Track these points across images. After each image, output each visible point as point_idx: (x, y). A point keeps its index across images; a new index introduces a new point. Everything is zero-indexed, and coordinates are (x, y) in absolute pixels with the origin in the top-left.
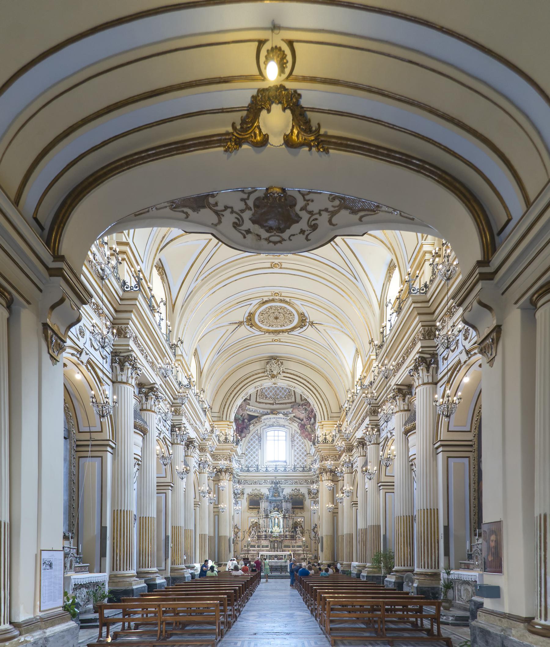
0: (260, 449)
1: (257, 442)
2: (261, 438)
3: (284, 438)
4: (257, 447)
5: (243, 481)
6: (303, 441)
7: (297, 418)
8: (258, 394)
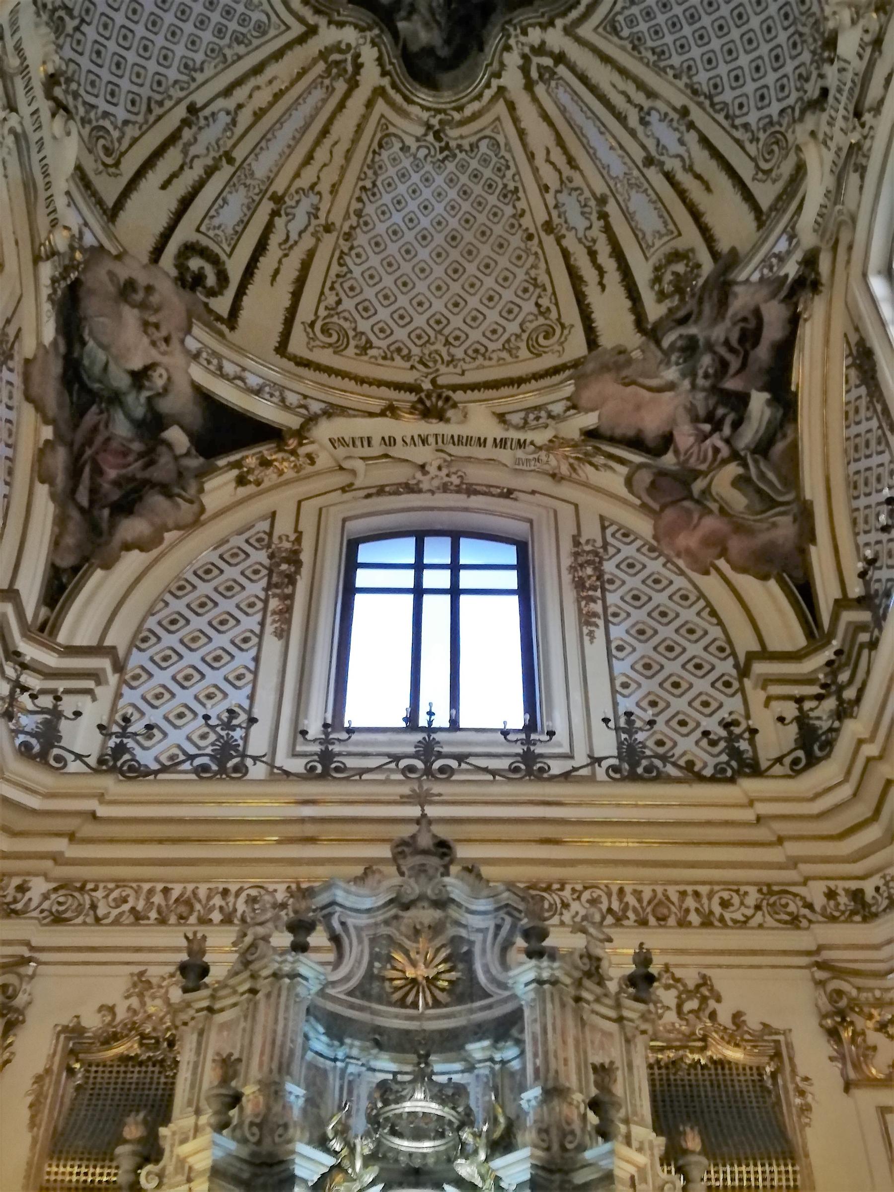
0: (283, 634)
1: (256, 588)
2: (298, 564)
3: (510, 579)
4: (251, 623)
5: (39, 887)
6: (680, 582)
7: (612, 440)
8: (305, 312)
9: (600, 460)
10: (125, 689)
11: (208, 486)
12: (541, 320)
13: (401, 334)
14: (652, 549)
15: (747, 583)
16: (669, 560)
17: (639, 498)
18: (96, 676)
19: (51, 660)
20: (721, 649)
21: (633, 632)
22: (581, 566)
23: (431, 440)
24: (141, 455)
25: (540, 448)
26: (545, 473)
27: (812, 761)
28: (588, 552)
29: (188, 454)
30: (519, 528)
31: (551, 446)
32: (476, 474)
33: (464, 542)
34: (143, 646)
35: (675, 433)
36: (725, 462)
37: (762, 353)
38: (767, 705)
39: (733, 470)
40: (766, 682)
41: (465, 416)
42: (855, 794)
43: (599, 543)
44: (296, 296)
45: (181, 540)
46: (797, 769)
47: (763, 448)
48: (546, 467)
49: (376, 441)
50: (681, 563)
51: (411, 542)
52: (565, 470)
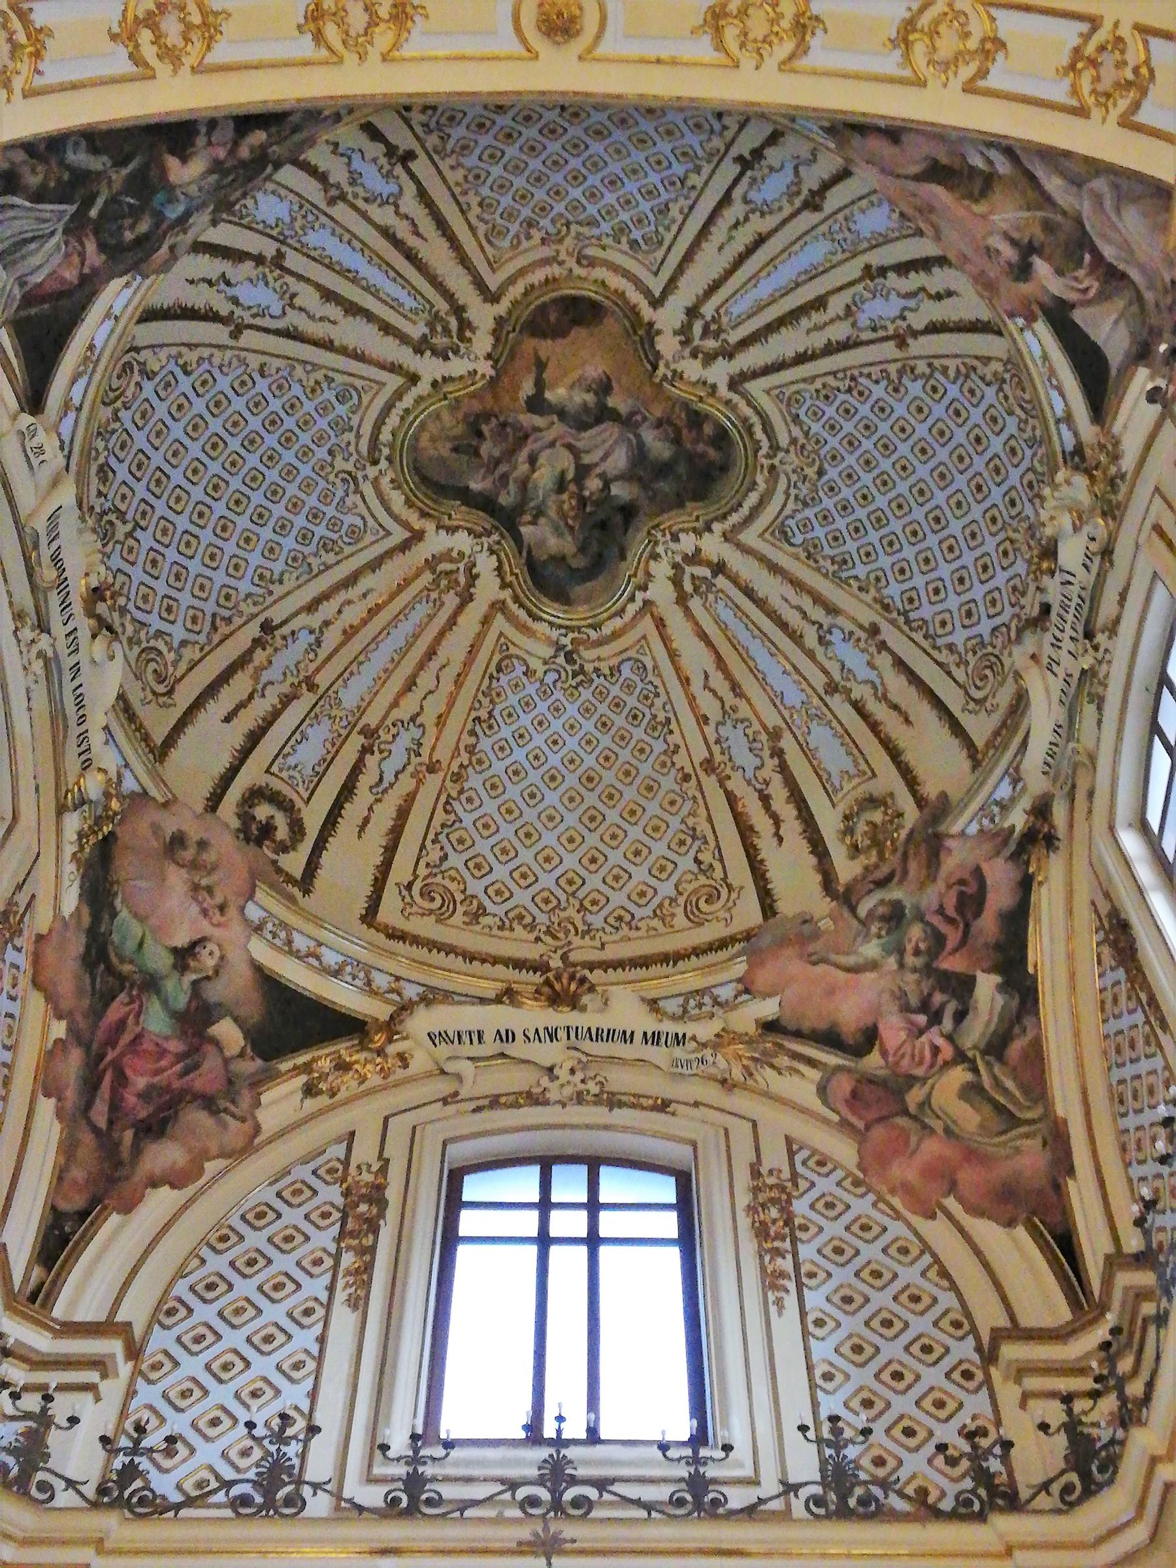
0: (359, 1303)
1: (324, 1239)
2: (382, 1204)
3: (668, 1224)
6: (897, 1229)
7: (798, 1035)
8: (401, 870)
9: (783, 1061)
10: (140, 1383)
11: (265, 1098)
12: (703, 880)
13: (522, 897)
14: (857, 1183)
15: (986, 1231)
16: (880, 1198)
17: (838, 1113)
18: (100, 1364)
19: (41, 1342)
20: (957, 1325)
21: (836, 1299)
22: (763, 1206)
23: (562, 1034)
24: (180, 1057)
25: (704, 1045)
26: (711, 1078)
27: (1090, 1489)
28: (771, 1188)
29: (242, 1055)
30: (679, 1154)
31: (720, 1041)
32: (621, 1080)
33: (604, 1171)
34: (168, 1321)
35: (881, 1027)
36: (947, 1065)
37: (988, 925)
38: (1023, 1405)
39: (959, 1075)
40: (1021, 1372)
41: (606, 1003)
42: (1154, 1536)
43: (786, 1174)
44: (390, 850)
45: (225, 1172)
46: (1069, 1502)
47: (996, 1047)
48: (712, 1070)
49: (489, 1036)
50: (896, 1202)
51: (534, 1171)
52: (737, 1074)
